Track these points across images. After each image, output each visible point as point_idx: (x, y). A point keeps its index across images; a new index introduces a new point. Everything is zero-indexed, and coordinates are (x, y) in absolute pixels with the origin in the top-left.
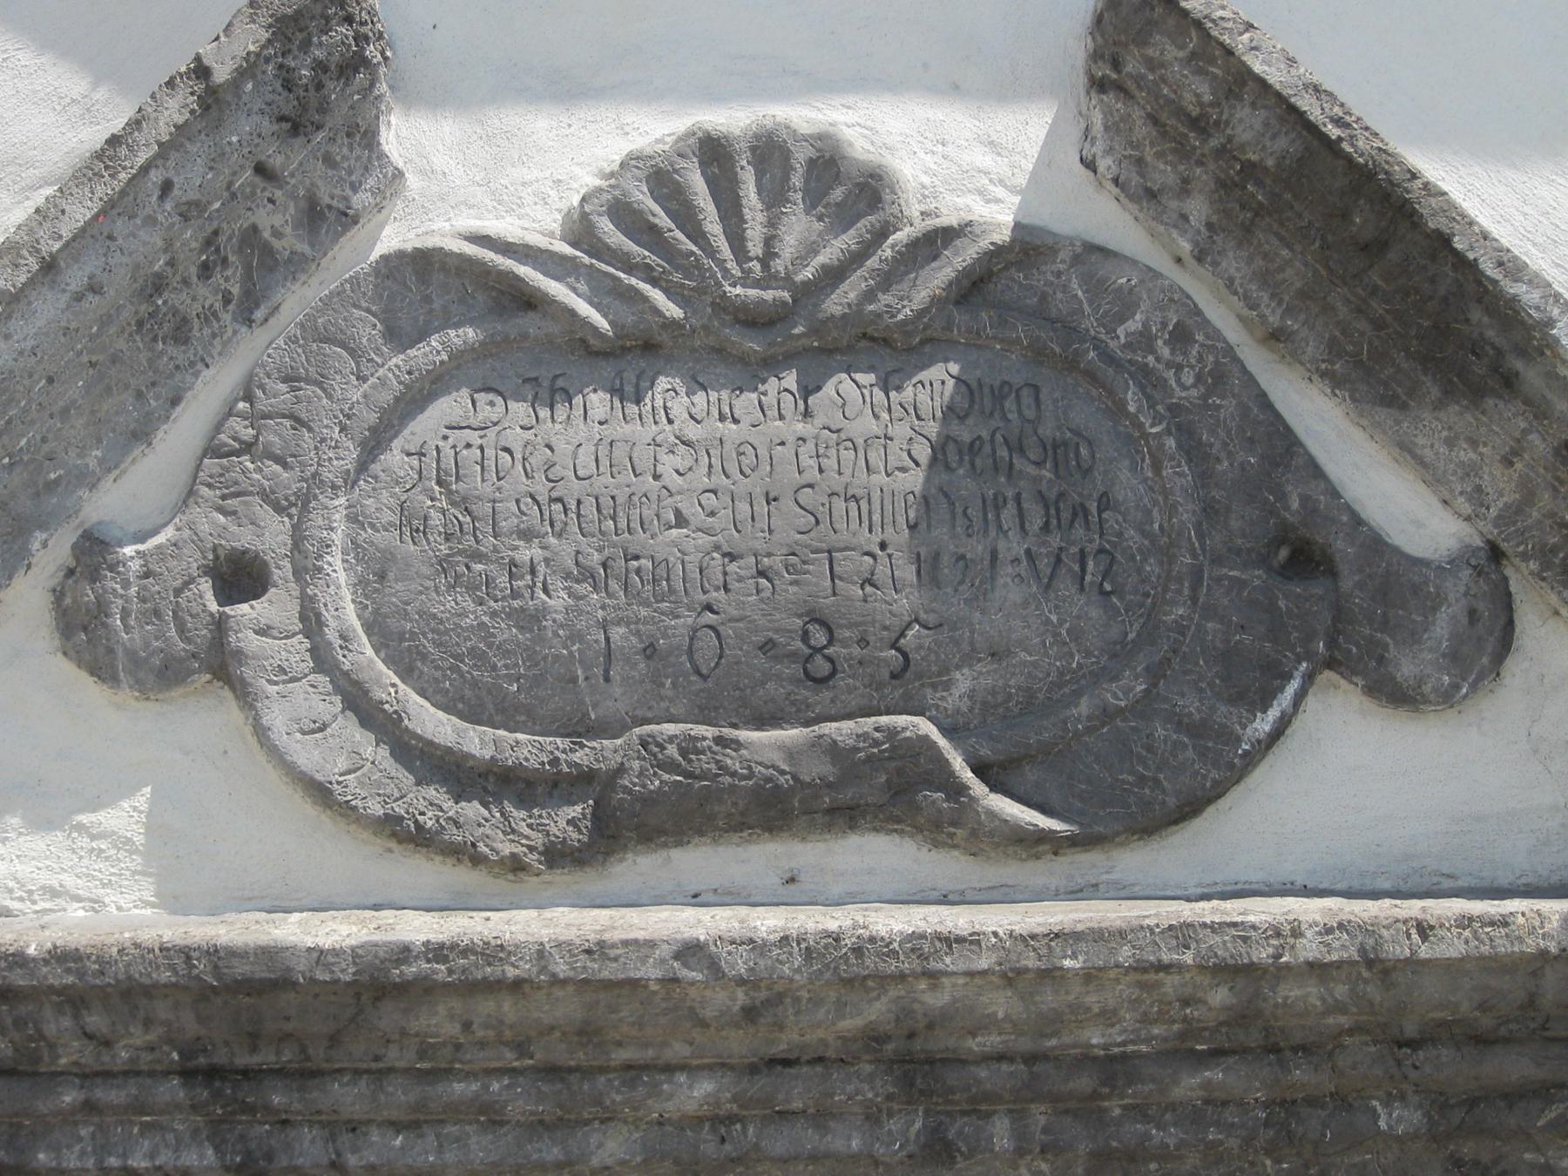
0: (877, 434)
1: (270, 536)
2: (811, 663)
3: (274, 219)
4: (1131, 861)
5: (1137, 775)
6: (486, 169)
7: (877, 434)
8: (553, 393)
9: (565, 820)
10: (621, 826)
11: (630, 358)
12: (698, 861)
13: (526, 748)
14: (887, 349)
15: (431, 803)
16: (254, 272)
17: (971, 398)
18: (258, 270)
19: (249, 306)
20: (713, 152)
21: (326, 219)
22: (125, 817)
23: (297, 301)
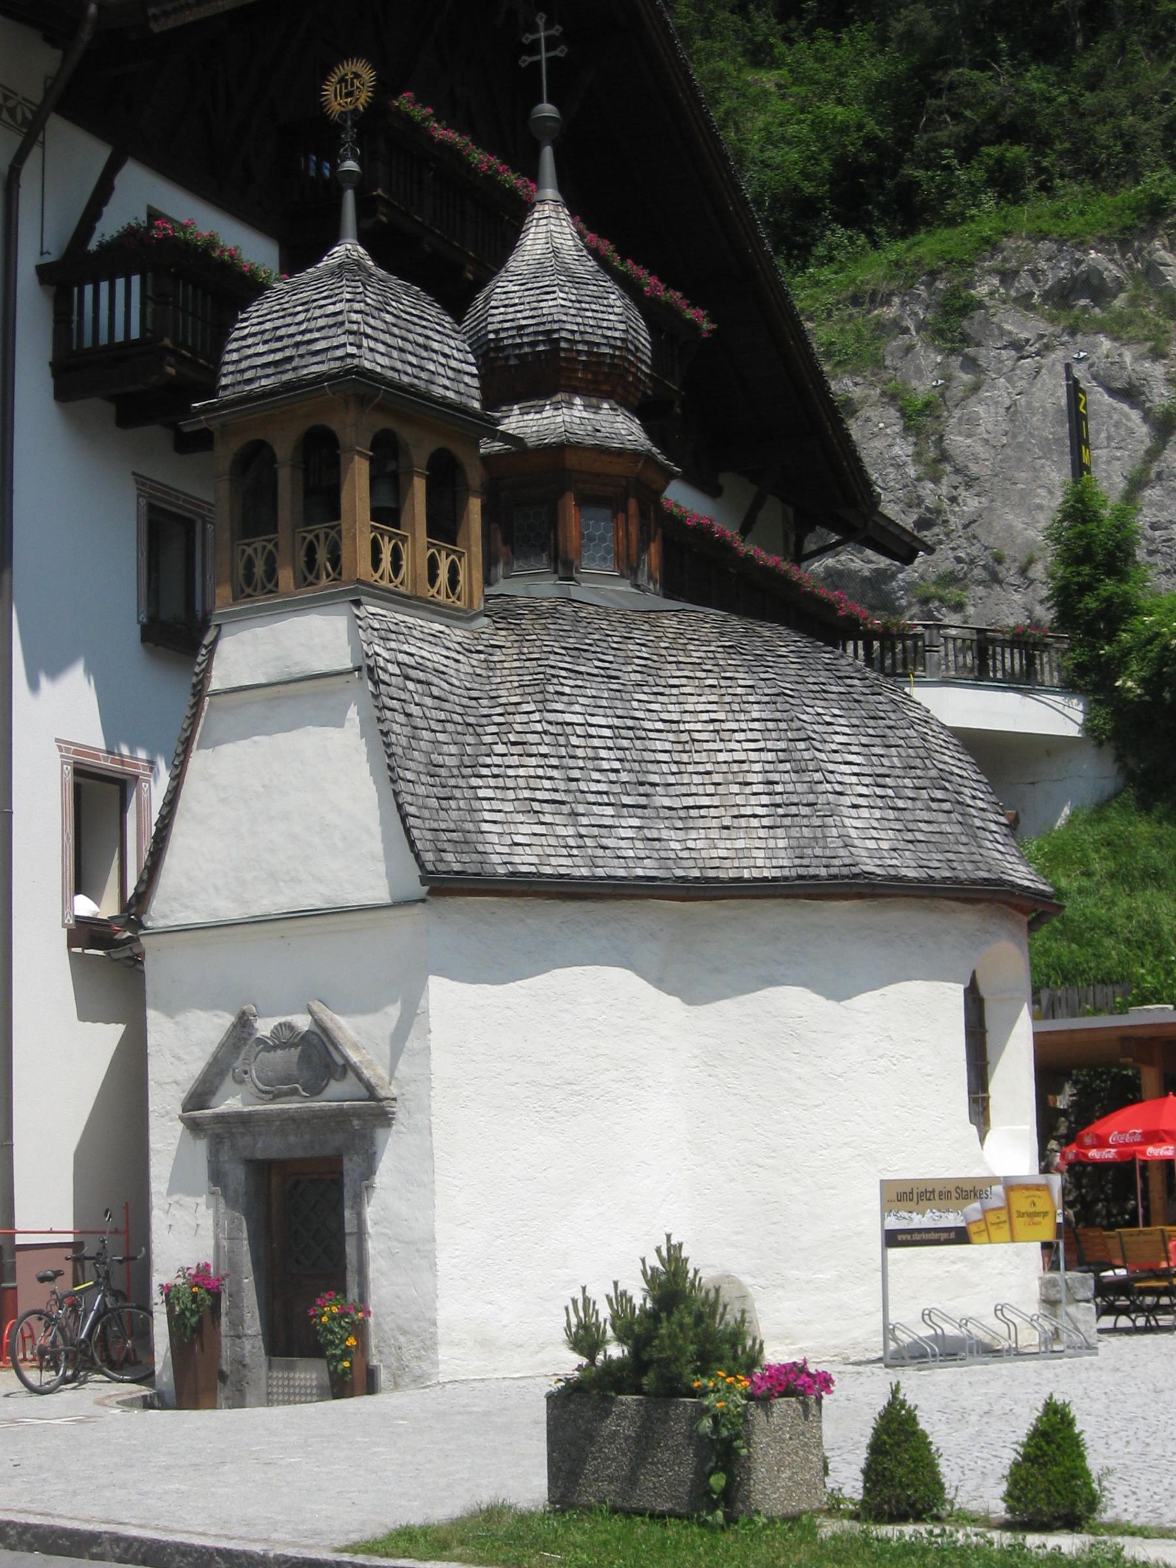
0: (295, 1053)
1: (247, 1068)
2: (288, 1080)
3: (245, 1035)
4: (319, 1097)
5: (315, 1090)
6: (264, 1027)
7: (295, 1053)
8: (269, 1051)
9: (271, 1096)
10: (276, 1096)
11: (275, 1048)
12: (283, 1099)
13: (268, 1088)
14: (295, 1045)
15: (261, 1095)
16: (245, 1040)
17: (302, 1051)
18: (245, 1040)
19: (245, 1044)
20: (280, 1024)
21: (250, 1034)
22: (239, 1097)
23: (249, 1042)
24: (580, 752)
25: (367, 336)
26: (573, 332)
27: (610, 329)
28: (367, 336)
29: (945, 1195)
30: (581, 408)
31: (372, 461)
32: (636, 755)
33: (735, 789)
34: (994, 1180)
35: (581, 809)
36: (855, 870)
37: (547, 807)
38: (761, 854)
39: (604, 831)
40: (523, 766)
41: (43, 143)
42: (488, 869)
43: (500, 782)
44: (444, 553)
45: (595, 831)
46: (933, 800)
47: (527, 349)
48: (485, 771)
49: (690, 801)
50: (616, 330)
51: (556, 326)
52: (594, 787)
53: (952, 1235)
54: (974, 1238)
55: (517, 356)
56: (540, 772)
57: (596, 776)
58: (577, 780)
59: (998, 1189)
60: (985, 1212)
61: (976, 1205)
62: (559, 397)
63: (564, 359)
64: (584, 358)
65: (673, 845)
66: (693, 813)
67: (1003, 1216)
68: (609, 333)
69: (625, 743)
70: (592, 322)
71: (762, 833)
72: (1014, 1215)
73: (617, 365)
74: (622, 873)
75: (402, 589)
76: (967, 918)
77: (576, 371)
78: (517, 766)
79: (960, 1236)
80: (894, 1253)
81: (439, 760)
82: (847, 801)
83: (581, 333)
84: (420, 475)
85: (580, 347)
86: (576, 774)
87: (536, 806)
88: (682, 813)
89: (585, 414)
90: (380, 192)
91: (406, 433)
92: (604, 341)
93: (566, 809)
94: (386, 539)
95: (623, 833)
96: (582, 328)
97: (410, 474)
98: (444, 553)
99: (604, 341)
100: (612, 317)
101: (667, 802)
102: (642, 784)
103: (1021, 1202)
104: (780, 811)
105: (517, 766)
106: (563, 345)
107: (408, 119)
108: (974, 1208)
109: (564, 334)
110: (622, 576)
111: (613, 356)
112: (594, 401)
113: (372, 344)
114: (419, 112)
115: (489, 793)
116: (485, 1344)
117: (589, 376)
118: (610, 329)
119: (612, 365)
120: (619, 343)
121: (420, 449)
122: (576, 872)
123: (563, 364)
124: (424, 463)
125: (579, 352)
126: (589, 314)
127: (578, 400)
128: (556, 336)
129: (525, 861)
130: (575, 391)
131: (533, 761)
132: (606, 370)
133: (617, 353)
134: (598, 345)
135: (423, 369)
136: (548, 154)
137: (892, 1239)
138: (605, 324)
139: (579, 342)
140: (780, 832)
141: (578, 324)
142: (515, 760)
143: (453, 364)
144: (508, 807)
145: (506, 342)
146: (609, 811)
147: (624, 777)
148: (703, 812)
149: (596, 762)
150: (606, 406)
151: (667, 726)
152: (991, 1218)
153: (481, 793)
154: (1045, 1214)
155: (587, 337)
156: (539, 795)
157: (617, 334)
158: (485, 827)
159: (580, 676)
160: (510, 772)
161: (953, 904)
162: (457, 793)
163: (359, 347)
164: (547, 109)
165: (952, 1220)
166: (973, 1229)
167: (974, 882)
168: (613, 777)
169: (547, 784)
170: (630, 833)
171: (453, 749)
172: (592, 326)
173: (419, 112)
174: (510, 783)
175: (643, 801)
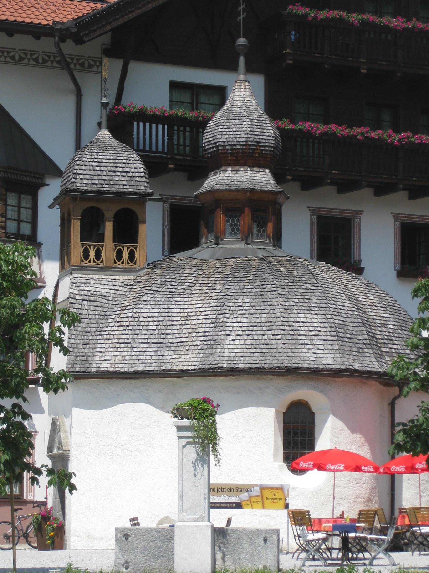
24: (142, 324)
25: (79, 174)
26: (224, 142)
27: (241, 138)
28: (79, 174)
29: (232, 490)
30: (230, 172)
31: (82, 221)
32: (164, 323)
33: (194, 334)
34: (256, 485)
35: (135, 345)
36: (217, 366)
37: (122, 345)
38: (190, 361)
39: (142, 353)
40: (118, 330)
41: (101, 72)
42: (89, 370)
43: (108, 337)
44: (126, 248)
45: (138, 353)
46: (273, 335)
47: (211, 150)
48: (103, 333)
49: (179, 340)
50: (243, 138)
51: (217, 140)
52: (143, 336)
53: (234, 505)
54: (244, 507)
55: (211, 153)
56: (124, 332)
57: (145, 332)
58: (138, 334)
59: (257, 489)
60: (250, 497)
61: (246, 494)
62: (223, 168)
63: (222, 153)
64: (230, 152)
65: (167, 357)
66: (179, 344)
67: (259, 499)
68: (240, 140)
69: (161, 319)
70: (232, 136)
71: (197, 352)
72: (265, 499)
73: (245, 152)
74: (140, 369)
75: (102, 265)
76: (280, 382)
77: (228, 157)
78: (116, 331)
79: (238, 506)
80: (212, 510)
81: (89, 330)
82: (230, 338)
83: (228, 142)
84: (109, 221)
85: (228, 147)
86: (137, 332)
87: (118, 345)
88: (175, 345)
89: (231, 175)
90: (288, 51)
91: (102, 206)
92: (238, 143)
93: (129, 346)
94: (92, 247)
95: (148, 354)
96: (228, 140)
97: (103, 222)
98: (126, 248)
99: (238, 143)
100: (242, 133)
101: (171, 341)
102: (163, 334)
103: (268, 494)
104: (205, 343)
105: (116, 331)
106: (220, 148)
107: (296, 15)
108: (244, 496)
109: (220, 143)
110: (242, 240)
111: (242, 149)
112: (237, 168)
113: (81, 176)
114: (301, 11)
115: (102, 341)
116: (89, 537)
117: (234, 158)
118: (241, 138)
119: (243, 153)
120: (244, 143)
121: (110, 211)
122: (123, 370)
123: (221, 155)
124: (112, 216)
125: (227, 150)
126: (232, 133)
127: (230, 169)
128: (217, 144)
129: (106, 366)
130: (229, 165)
131: (122, 328)
132: (241, 155)
133: (244, 147)
134: (235, 145)
135: (111, 180)
136: (242, 60)
137: (214, 505)
138: (238, 136)
139: (227, 145)
140: (202, 351)
141: (226, 138)
142: (115, 328)
143: (130, 174)
144: (107, 346)
145: (207, 147)
146: (147, 345)
147: (156, 332)
148: (182, 344)
149: (147, 327)
150: (242, 169)
151: (182, 311)
152: (253, 499)
153: (99, 341)
154: (280, 499)
155: (230, 143)
156: (120, 341)
157: (243, 140)
158: (96, 354)
159: (158, 293)
160: (113, 333)
161: (271, 376)
162: (91, 342)
163: (76, 179)
164: (242, 41)
165: (234, 499)
166: (244, 503)
167: (271, 368)
168: (152, 332)
169: (125, 337)
170: (151, 354)
171: (95, 325)
172: (232, 138)
173: (301, 11)
174: (112, 337)
175: (161, 341)
